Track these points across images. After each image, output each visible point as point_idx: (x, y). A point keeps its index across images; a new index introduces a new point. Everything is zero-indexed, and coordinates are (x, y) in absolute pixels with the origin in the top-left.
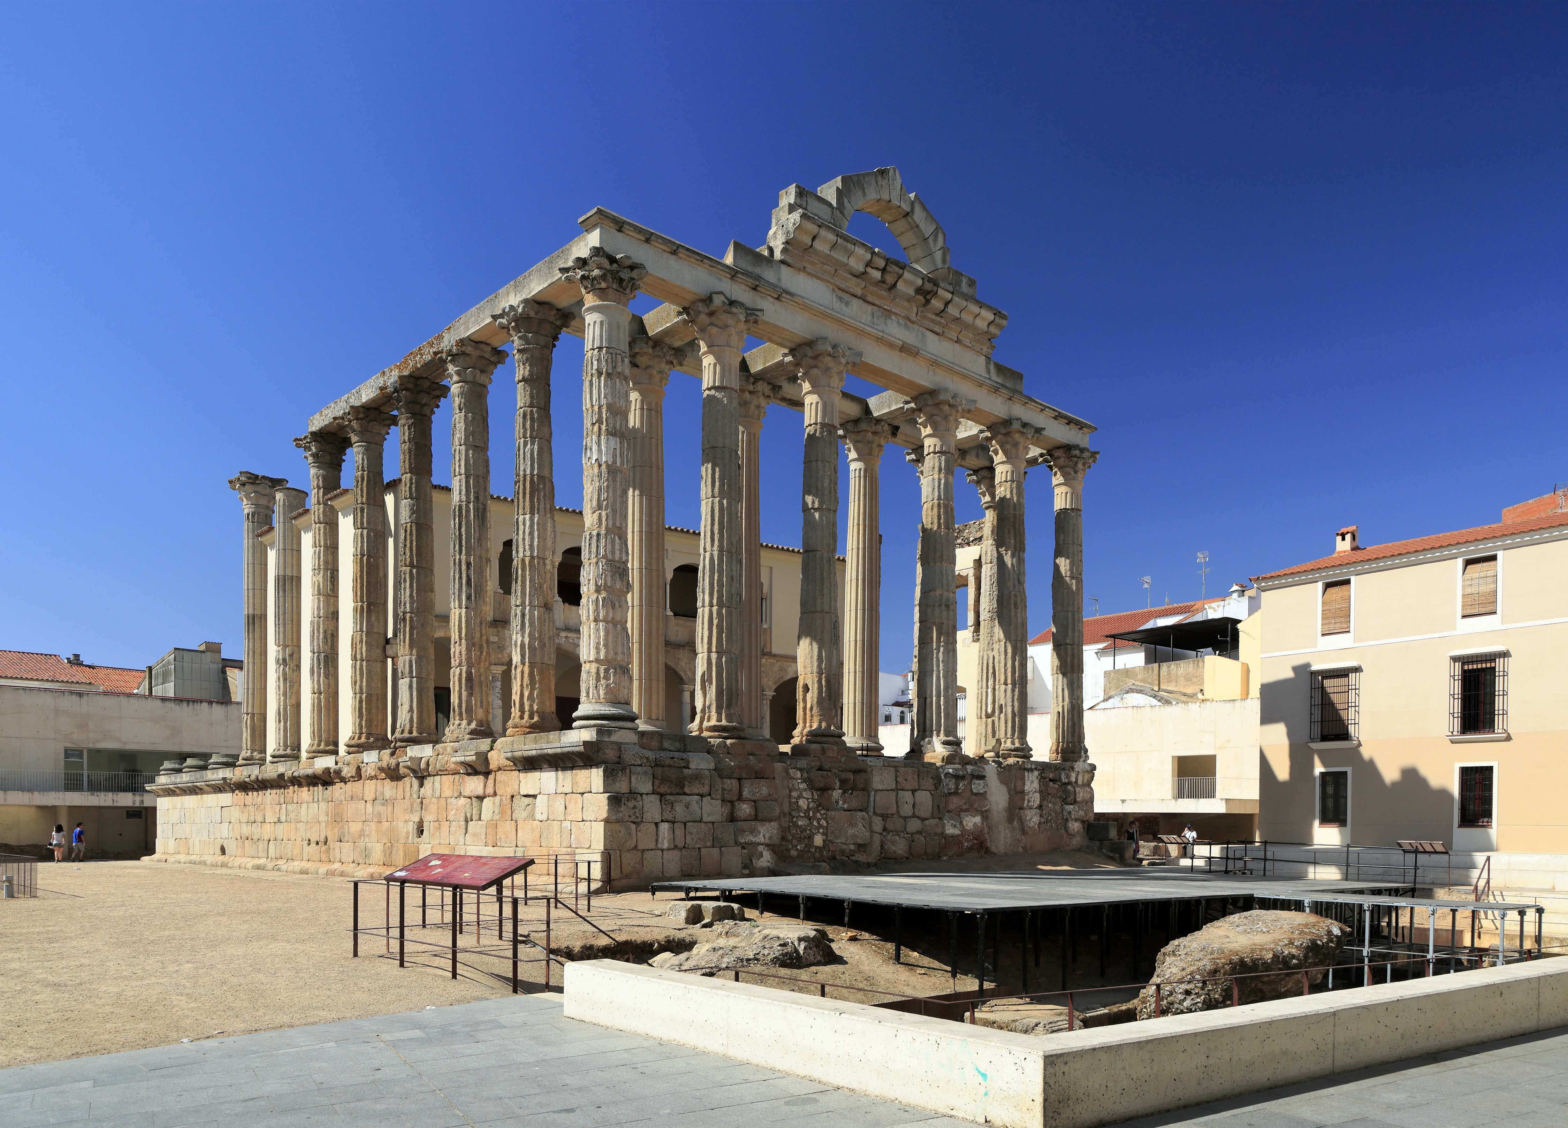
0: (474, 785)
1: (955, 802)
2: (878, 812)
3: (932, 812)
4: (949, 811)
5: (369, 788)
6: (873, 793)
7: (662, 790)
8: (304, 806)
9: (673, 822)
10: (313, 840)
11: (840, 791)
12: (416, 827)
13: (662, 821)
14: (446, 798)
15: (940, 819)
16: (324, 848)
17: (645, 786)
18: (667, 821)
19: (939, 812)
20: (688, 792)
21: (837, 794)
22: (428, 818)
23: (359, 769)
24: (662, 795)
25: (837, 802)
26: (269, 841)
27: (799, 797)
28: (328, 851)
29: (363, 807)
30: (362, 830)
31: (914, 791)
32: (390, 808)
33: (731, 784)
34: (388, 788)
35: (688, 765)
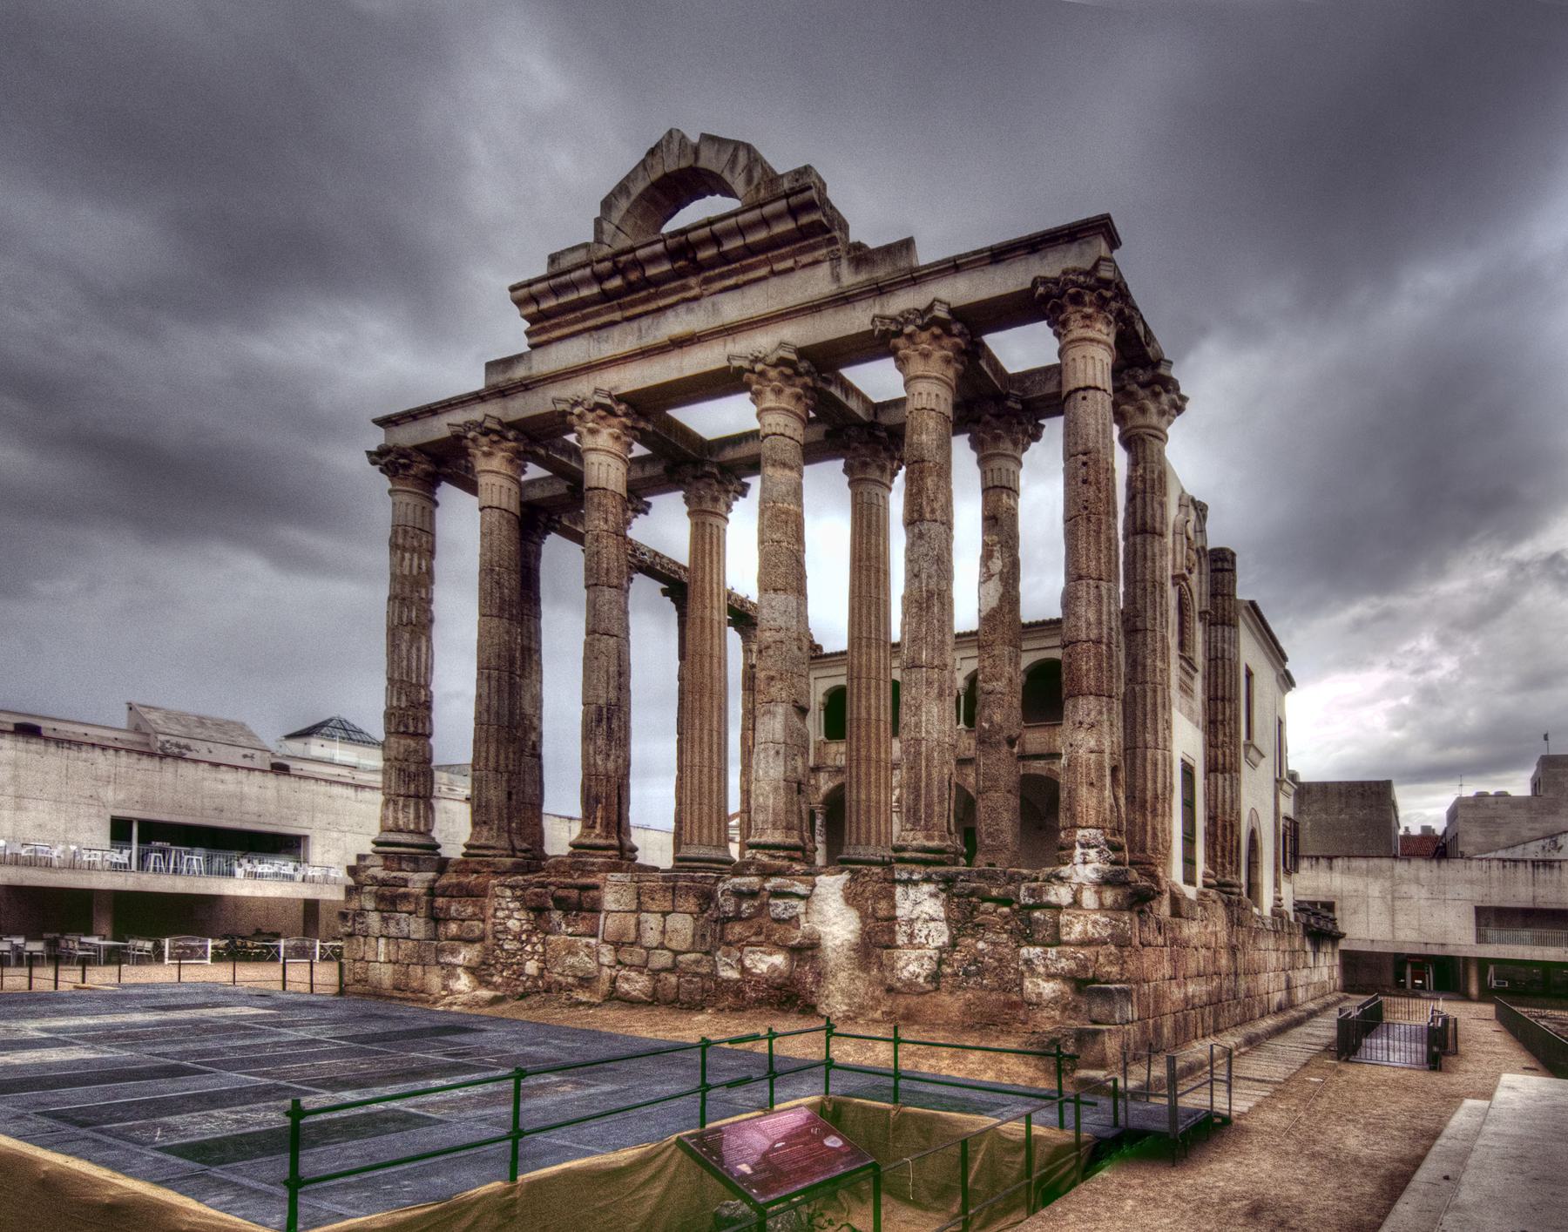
1: (737, 930)
3: (693, 943)
6: (602, 916)
7: (381, 907)
9: (388, 937)
11: (559, 912)
15: (707, 953)
21: (556, 916)
25: (559, 925)
27: (509, 917)
31: (665, 914)
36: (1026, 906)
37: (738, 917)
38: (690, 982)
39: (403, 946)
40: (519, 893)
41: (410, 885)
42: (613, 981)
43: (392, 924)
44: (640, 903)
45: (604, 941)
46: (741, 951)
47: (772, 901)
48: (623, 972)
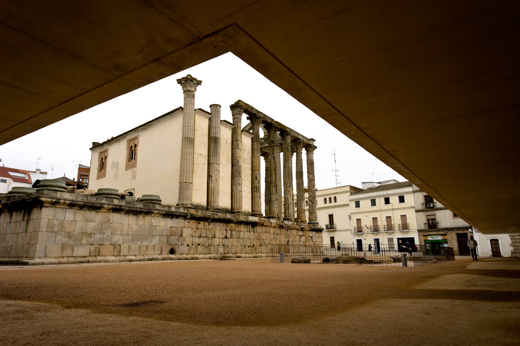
0: (301, 233)
5: (272, 230)
8: (242, 233)
10: (247, 244)
28: (255, 249)
29: (270, 235)
30: (269, 243)
32: (279, 237)
34: (278, 231)
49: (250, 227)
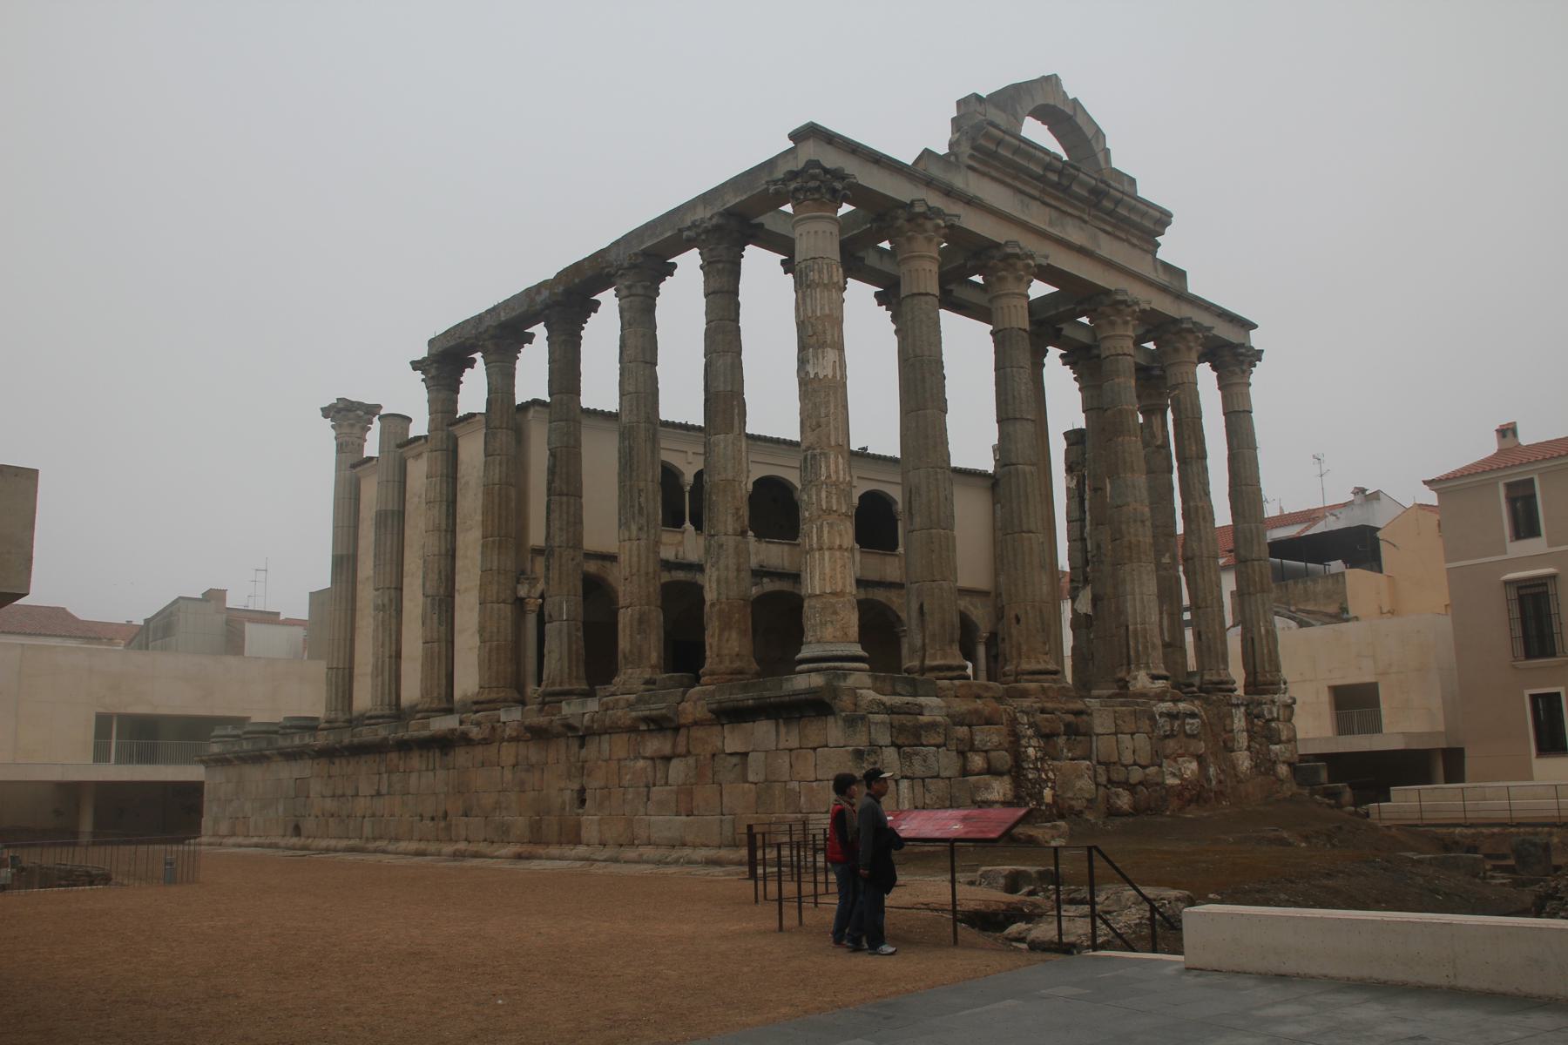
0: (656, 744)
1: (1171, 744)
2: (1101, 760)
4: (1167, 757)
5: (508, 753)
6: (1094, 738)
7: (899, 742)
8: (414, 777)
11: (1064, 737)
12: (575, 795)
13: (902, 778)
14: (619, 760)
16: (442, 824)
17: (884, 739)
18: (907, 778)
19: (1157, 757)
20: (925, 743)
21: (1061, 741)
22: (593, 784)
23: (493, 729)
24: (899, 747)
25: (1062, 750)
26: (364, 817)
28: (448, 828)
33: (962, 731)
34: (533, 753)
35: (922, 712)
36: (1268, 721)
37: (1171, 736)
38: (1156, 791)
39: (932, 788)
40: (1032, 720)
41: (926, 712)
42: (1108, 798)
43: (917, 761)
44: (1116, 725)
45: (1099, 763)
46: (1176, 761)
47: (1189, 720)
48: (1113, 790)
49: (438, 754)
